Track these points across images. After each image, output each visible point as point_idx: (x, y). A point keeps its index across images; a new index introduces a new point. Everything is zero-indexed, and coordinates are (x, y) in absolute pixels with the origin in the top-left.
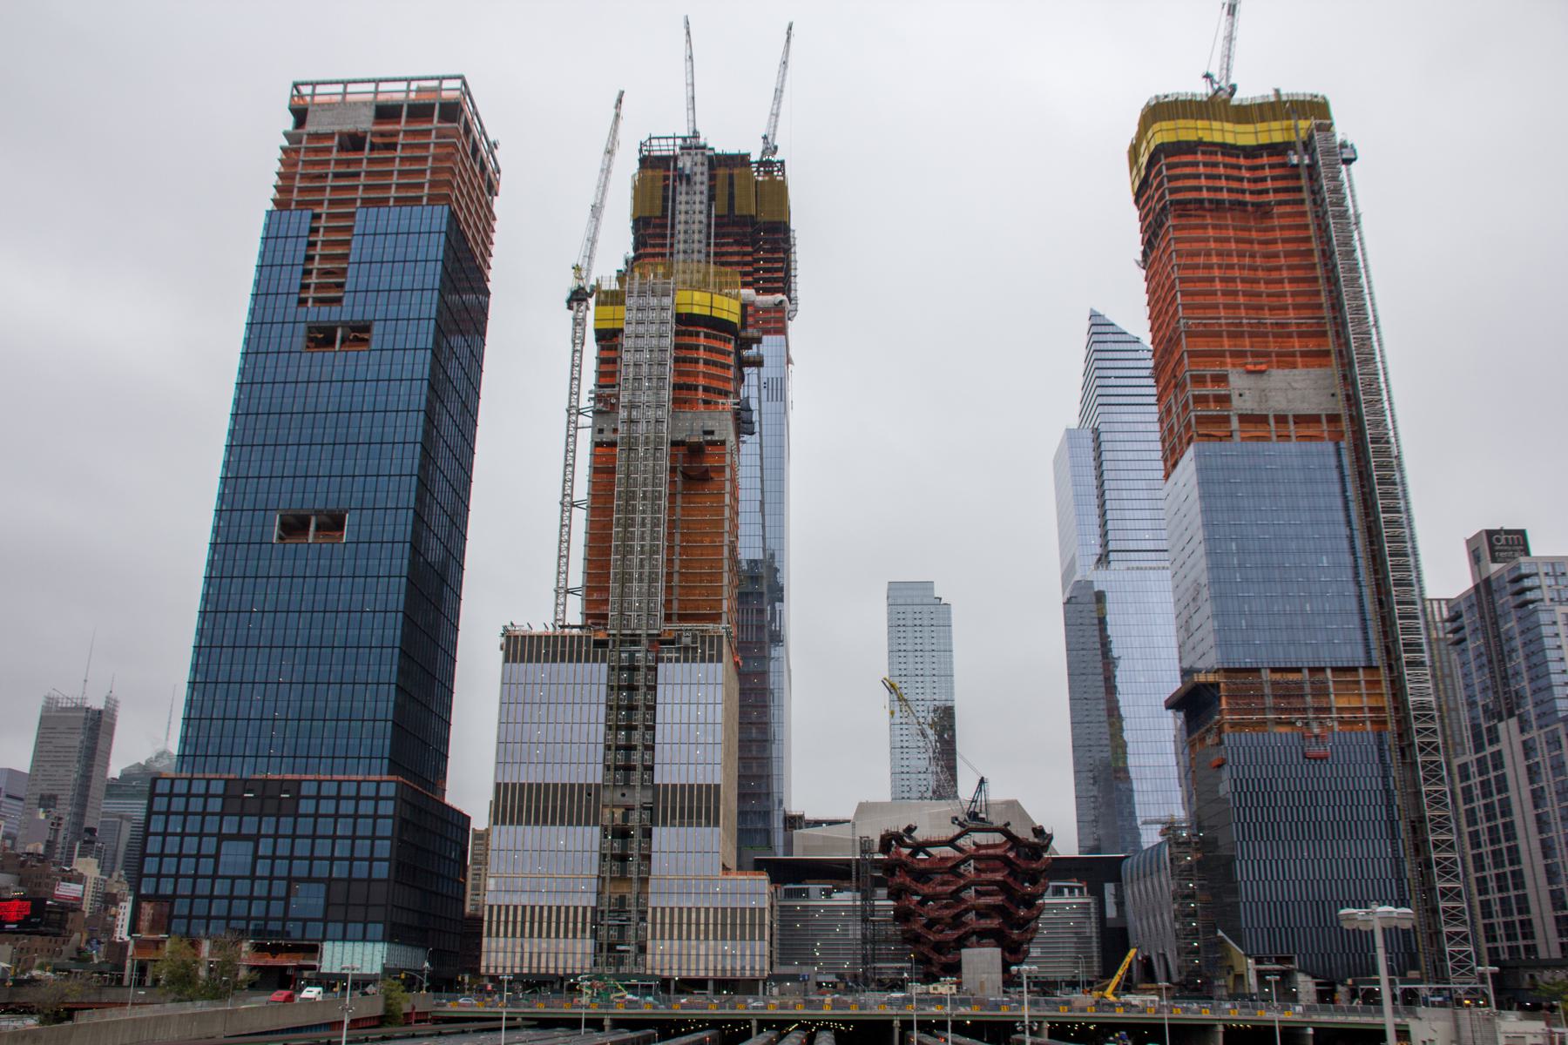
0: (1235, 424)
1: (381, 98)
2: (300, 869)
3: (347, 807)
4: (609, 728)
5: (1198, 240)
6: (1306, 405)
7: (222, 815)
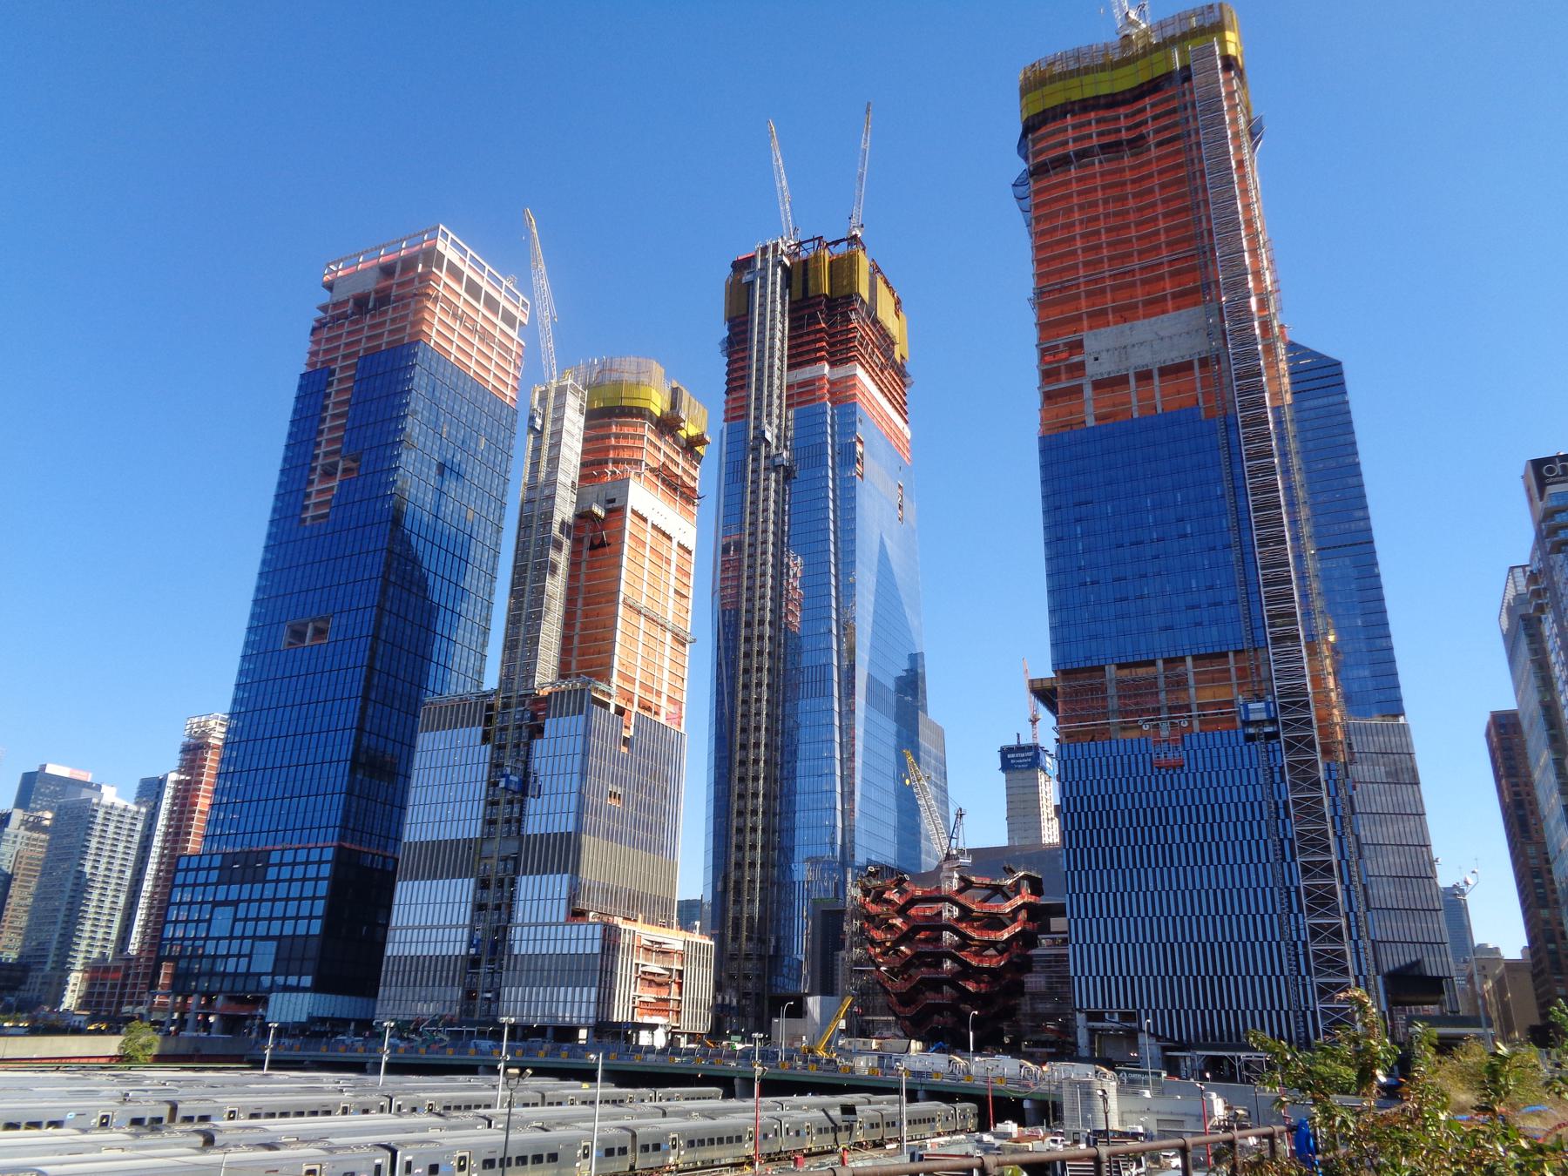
0: (1088, 392)
2: (262, 929)
6: (1174, 354)
7: (217, 884)
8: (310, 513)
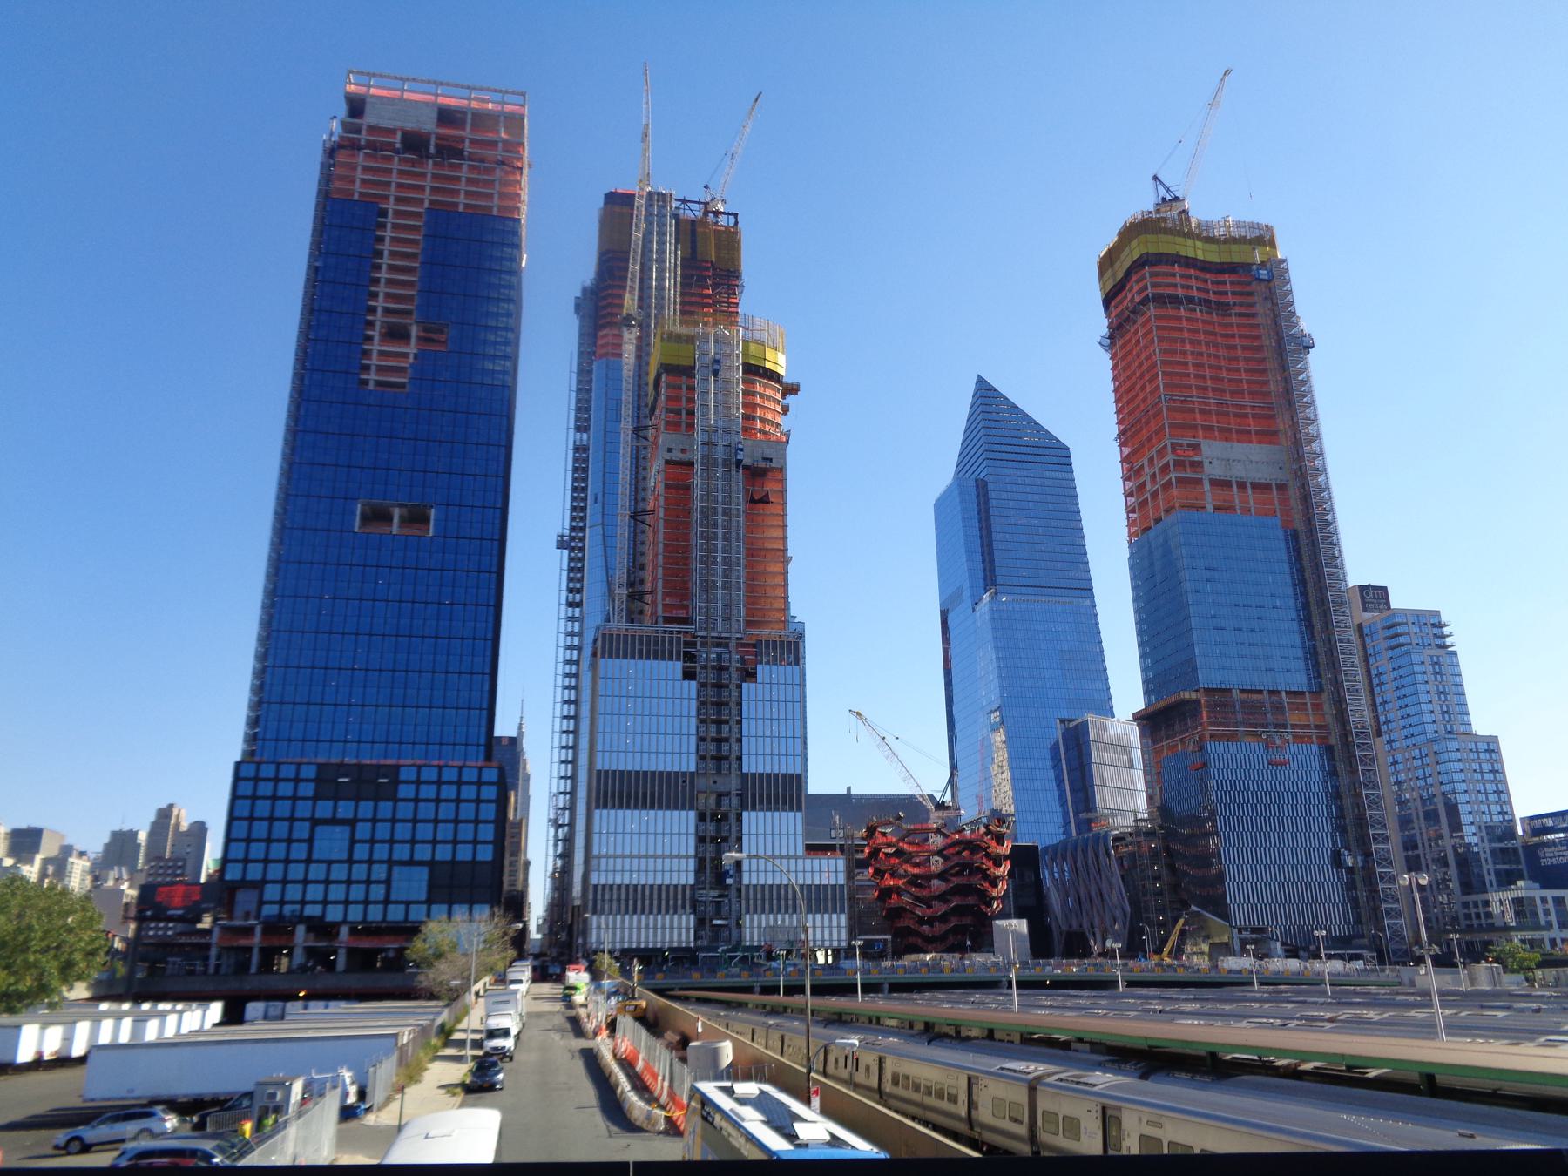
0: (1207, 486)
1: (441, 100)
2: (402, 852)
3: (449, 792)
4: (701, 721)
5: (1172, 329)
7: (316, 798)
8: (373, 376)
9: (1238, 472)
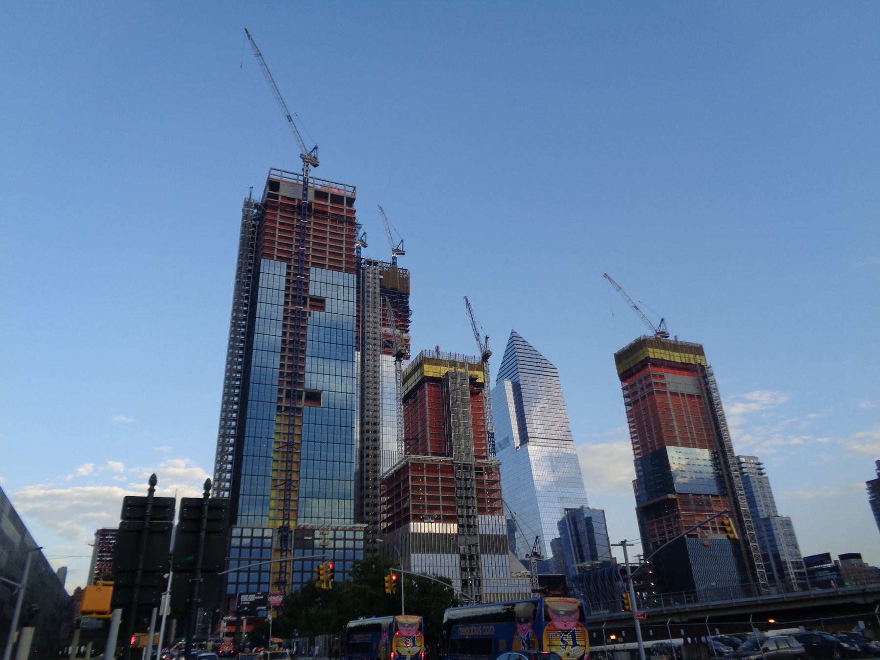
9: (681, 389)
